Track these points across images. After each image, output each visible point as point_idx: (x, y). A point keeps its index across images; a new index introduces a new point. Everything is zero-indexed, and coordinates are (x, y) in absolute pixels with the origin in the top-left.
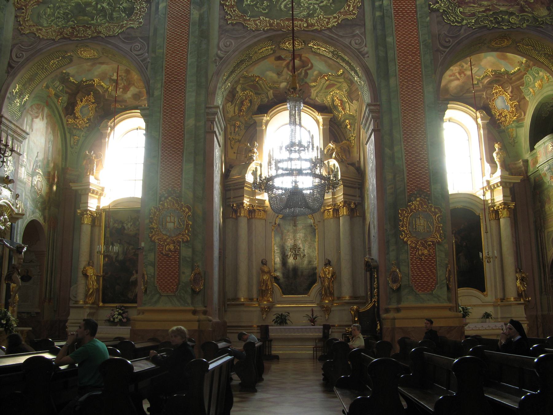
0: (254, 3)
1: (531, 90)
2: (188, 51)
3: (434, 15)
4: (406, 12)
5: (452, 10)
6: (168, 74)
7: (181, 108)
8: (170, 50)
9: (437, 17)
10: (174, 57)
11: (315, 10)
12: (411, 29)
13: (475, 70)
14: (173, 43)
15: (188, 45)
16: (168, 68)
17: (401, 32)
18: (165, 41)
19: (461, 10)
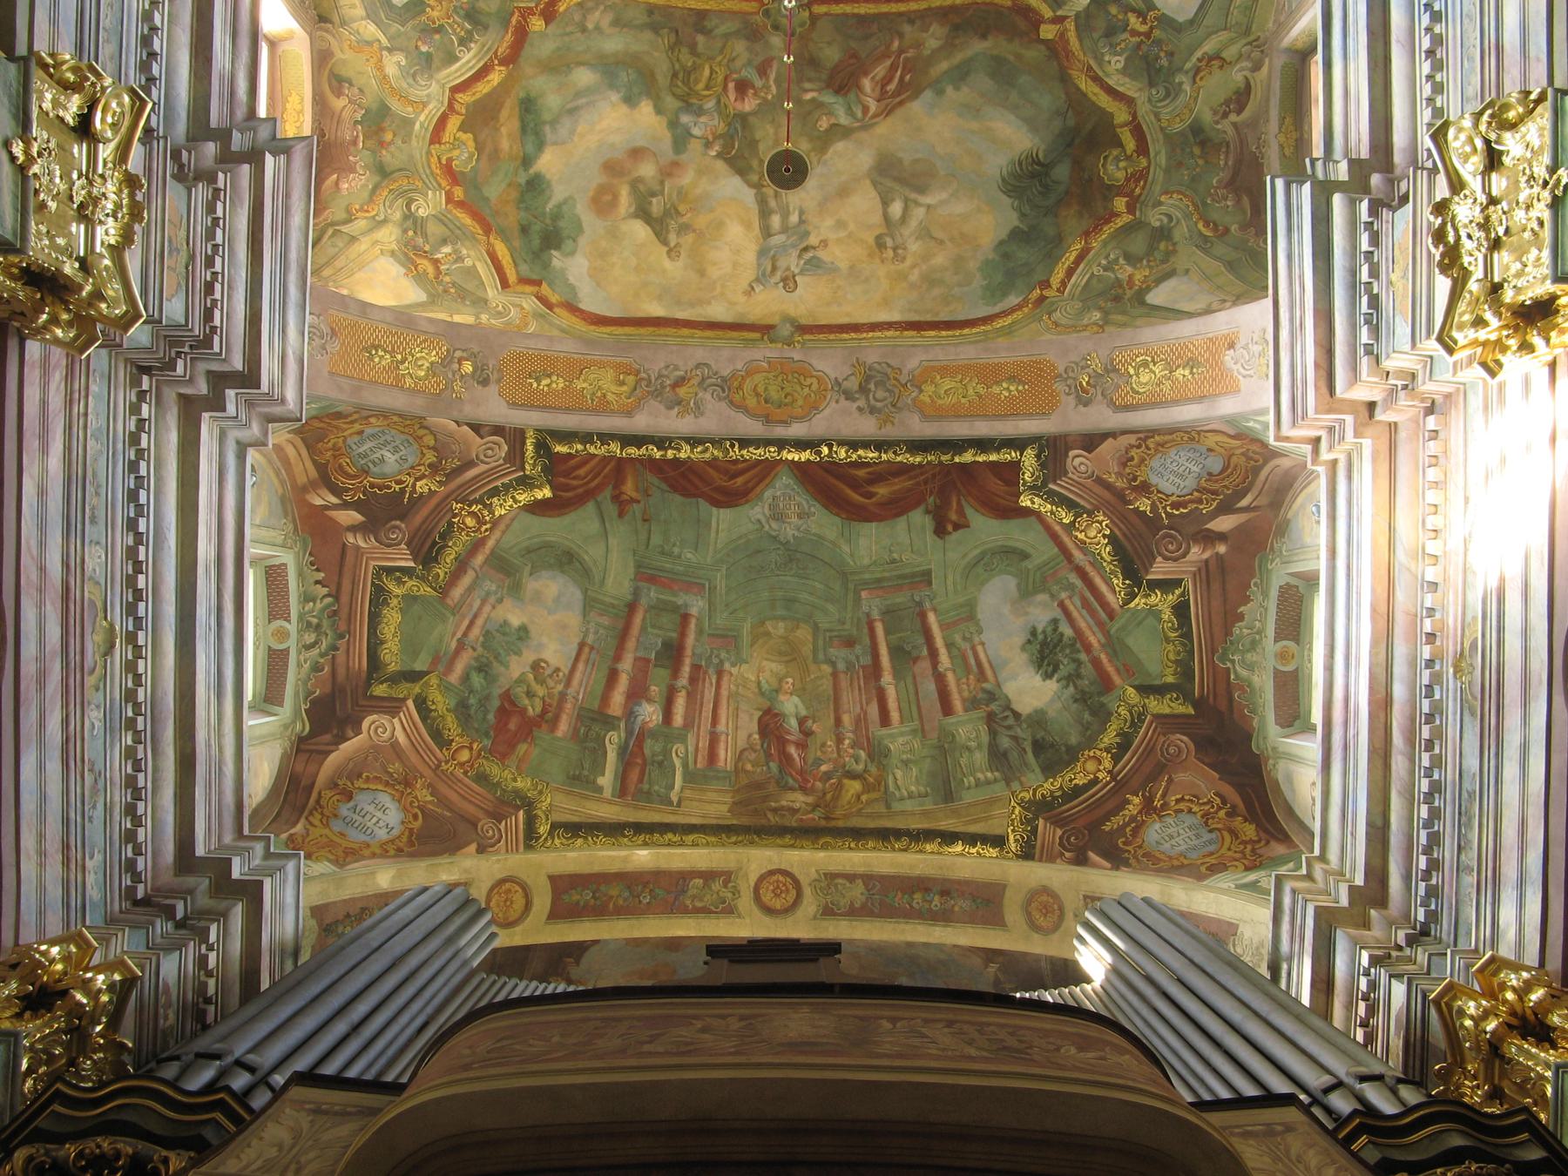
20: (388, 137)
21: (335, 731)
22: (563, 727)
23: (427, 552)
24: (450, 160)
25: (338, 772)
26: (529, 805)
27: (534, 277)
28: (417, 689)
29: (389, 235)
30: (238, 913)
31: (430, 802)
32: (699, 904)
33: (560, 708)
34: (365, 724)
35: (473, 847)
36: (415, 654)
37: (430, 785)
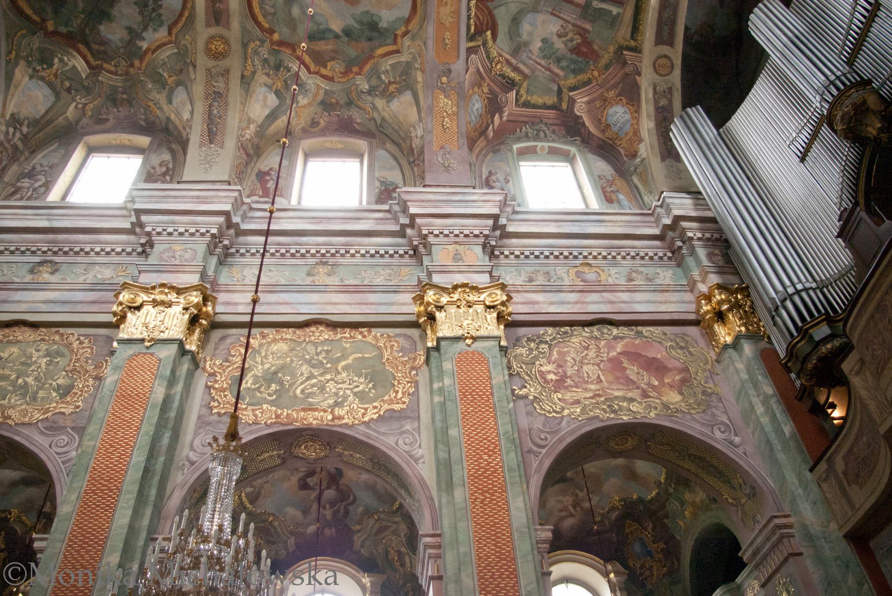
0: (257, 386)
1: (681, 523)
2: (135, 445)
3: (521, 403)
4: (477, 394)
5: (546, 396)
6: (94, 479)
7: (102, 535)
8: (106, 443)
9: (526, 405)
10: (110, 453)
11: (345, 398)
12: (485, 417)
13: (595, 500)
14: (115, 433)
15: (138, 436)
16: (95, 470)
17: (471, 422)
18: (103, 429)
19: (560, 396)
20: (333, 101)
22: (588, 26)
23: (511, 84)
24: (340, 72)
26: (621, 48)
27: (393, 37)
28: (566, 90)
29: (380, 103)
30: (685, 224)
33: (579, 27)
34: (578, 114)
35: (637, 77)
36: (550, 90)
37: (607, 90)
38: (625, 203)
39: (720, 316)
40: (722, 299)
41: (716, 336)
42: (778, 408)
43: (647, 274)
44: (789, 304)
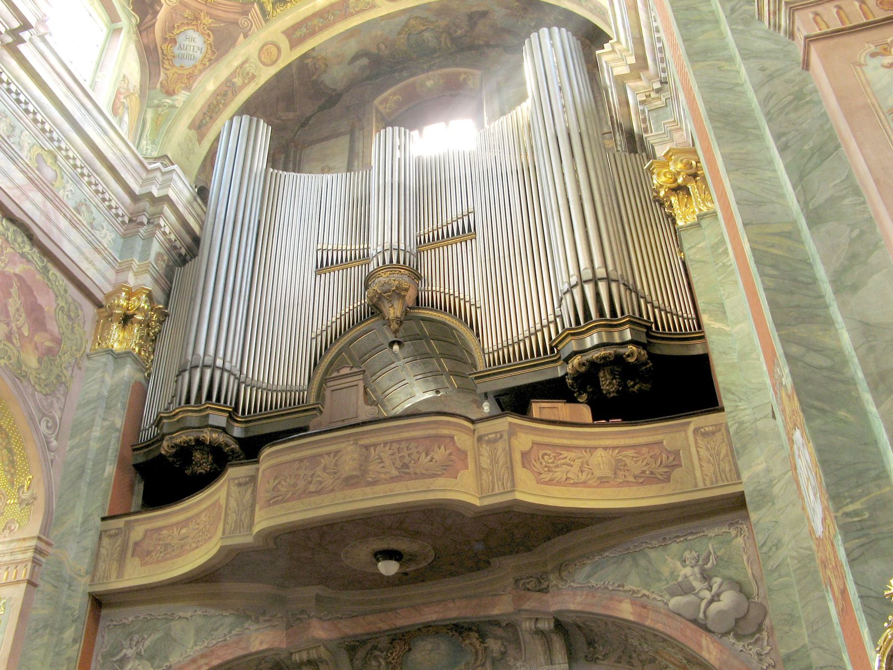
21: (151, 12)
25: (164, 32)
30: (167, 210)
31: (211, 23)
32: (358, 9)
35: (242, 35)
38: (125, 127)
39: (126, 319)
40: (143, 307)
41: (108, 334)
42: (114, 445)
43: (94, 219)
44: (208, 372)
